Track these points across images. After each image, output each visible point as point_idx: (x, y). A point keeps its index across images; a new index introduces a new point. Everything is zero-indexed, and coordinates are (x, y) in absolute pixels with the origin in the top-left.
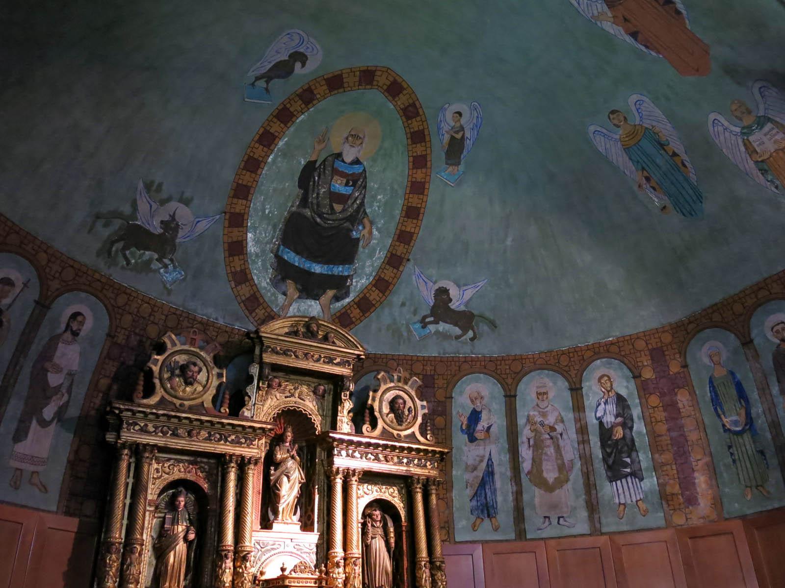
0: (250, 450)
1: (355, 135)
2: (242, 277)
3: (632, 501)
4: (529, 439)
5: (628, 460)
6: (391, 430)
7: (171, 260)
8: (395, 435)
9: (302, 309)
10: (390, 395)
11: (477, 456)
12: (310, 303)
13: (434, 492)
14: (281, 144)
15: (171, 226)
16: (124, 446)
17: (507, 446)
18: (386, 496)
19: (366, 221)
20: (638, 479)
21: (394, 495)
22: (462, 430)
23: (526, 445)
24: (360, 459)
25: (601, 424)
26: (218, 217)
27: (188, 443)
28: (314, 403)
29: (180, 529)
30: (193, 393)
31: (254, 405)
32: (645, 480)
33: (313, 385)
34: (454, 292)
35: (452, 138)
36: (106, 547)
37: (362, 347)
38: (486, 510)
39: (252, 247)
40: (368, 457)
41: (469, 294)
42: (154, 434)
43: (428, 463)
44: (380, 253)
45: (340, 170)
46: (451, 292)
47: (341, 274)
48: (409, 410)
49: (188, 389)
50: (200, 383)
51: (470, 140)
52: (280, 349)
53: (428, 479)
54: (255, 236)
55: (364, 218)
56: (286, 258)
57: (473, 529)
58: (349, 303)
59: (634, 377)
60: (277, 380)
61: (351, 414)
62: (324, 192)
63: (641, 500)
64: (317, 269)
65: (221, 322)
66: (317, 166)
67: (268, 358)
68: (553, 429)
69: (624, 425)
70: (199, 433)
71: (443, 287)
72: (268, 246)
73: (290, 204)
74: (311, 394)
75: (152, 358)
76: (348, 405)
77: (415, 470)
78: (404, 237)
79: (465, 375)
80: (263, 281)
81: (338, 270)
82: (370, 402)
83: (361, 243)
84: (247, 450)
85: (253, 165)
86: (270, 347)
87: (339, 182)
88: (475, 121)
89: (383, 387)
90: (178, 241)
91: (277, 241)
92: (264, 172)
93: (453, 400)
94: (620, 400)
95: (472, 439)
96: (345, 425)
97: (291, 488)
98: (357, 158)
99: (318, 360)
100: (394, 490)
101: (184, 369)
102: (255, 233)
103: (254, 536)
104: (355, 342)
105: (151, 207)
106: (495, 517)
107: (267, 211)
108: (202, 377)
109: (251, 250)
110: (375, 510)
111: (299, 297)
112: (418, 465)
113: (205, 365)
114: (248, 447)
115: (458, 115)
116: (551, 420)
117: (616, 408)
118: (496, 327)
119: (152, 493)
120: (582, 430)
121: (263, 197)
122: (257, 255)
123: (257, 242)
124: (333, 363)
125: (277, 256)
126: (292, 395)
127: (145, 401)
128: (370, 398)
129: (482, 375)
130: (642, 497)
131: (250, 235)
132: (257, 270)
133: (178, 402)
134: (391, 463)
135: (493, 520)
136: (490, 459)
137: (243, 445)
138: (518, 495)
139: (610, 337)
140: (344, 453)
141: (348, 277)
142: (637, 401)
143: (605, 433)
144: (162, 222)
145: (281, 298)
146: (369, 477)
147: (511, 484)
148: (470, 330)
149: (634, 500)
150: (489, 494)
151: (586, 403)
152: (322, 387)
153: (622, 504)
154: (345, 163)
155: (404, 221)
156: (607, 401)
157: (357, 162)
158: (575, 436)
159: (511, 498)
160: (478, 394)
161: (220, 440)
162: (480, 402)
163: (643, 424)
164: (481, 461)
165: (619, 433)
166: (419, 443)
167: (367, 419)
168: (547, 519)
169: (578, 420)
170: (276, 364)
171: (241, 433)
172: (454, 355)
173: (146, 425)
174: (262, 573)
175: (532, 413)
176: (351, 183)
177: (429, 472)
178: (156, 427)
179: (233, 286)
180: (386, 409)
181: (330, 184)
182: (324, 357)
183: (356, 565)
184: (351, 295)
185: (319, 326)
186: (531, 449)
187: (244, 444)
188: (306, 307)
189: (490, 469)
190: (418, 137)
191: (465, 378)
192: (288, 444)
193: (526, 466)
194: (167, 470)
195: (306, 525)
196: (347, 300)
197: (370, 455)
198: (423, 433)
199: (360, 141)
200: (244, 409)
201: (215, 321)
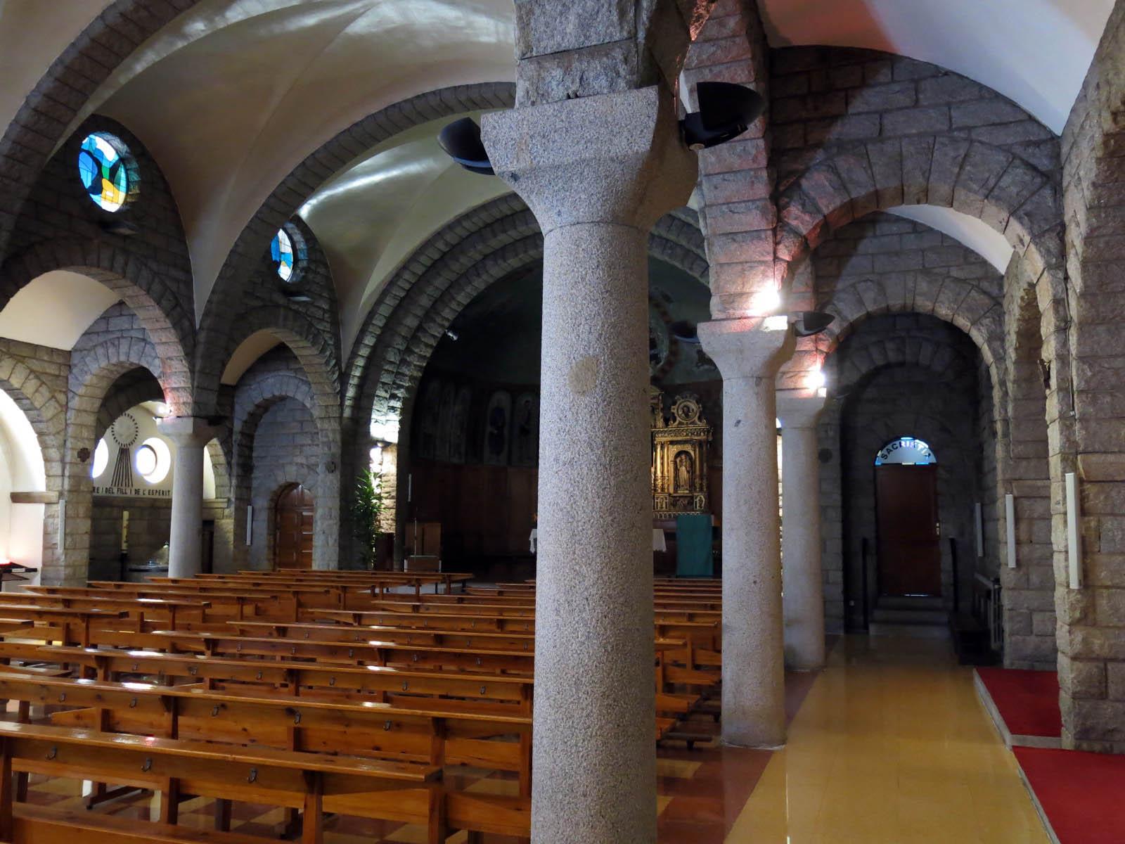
10: (682, 405)
18: (686, 449)
76: (661, 414)
89: (678, 403)
96: (660, 423)
112: (697, 435)
141: (657, 355)
180: (680, 413)
196: (661, 364)
198: (700, 418)
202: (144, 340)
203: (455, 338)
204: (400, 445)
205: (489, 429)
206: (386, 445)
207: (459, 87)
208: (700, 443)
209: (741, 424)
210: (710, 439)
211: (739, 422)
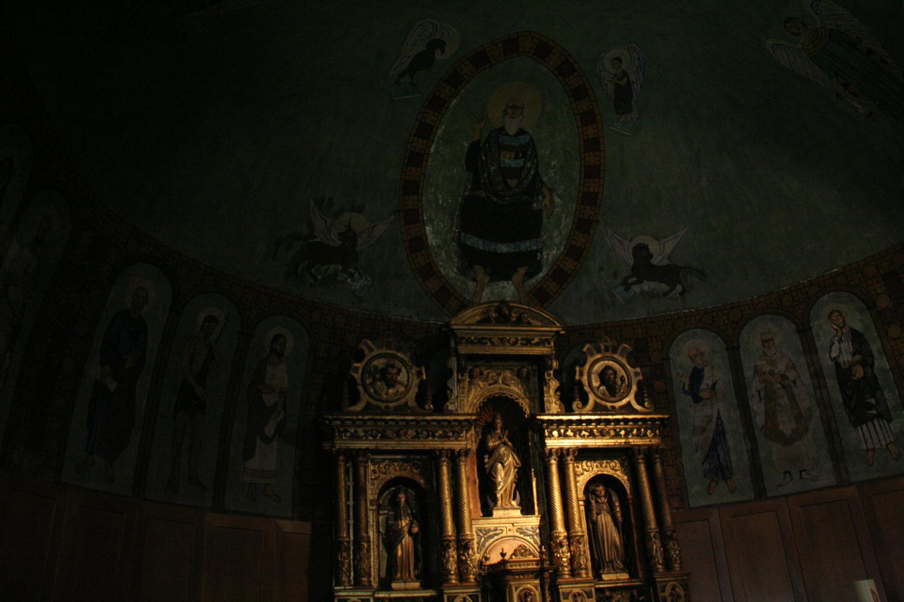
0: (458, 443)
1: (513, 106)
2: (429, 271)
3: (881, 445)
4: (759, 392)
5: (873, 401)
6: (603, 403)
7: (356, 269)
8: (609, 408)
9: (495, 292)
10: (598, 367)
11: (705, 416)
12: (502, 285)
13: (658, 460)
14: (439, 132)
15: (349, 236)
16: (340, 452)
17: (736, 402)
18: (608, 471)
19: (544, 190)
20: (886, 420)
21: (617, 468)
22: (685, 392)
23: (757, 399)
24: (573, 437)
25: (837, 365)
26: (392, 217)
27: (398, 443)
28: (520, 386)
29: (404, 523)
30: (396, 395)
31: (457, 397)
32: (894, 421)
33: (516, 369)
34: (653, 247)
35: (616, 85)
36: (337, 546)
37: (558, 322)
39: (432, 240)
40: (582, 434)
41: (670, 245)
42: (364, 438)
43: (649, 432)
44: (566, 220)
45: (506, 144)
46: (650, 247)
47: (529, 249)
48: (622, 379)
49: (391, 391)
50: (401, 384)
51: (637, 84)
52: (475, 338)
53: (650, 447)
54: (433, 228)
55: (541, 188)
56: (469, 243)
57: (709, 494)
58: (543, 278)
59: (869, 308)
60: (478, 370)
61: (558, 393)
62: (494, 170)
63: (891, 442)
64: (504, 248)
65: (416, 319)
66: (481, 146)
67: (464, 350)
68: (784, 377)
69: (863, 363)
70: (406, 433)
71: (640, 244)
72: (449, 235)
73: (462, 190)
74: (515, 377)
75: (353, 367)
76: (554, 384)
78: (589, 199)
79: (681, 333)
80: (450, 271)
81: (525, 246)
82: (577, 377)
83: (544, 214)
84: (455, 443)
85: (416, 159)
86: (464, 338)
87: (508, 156)
88: (637, 63)
89: (590, 360)
90: (358, 249)
91: (457, 229)
92: (429, 164)
93: (671, 361)
94: (857, 337)
95: (697, 399)
96: (554, 405)
97: (507, 474)
98: (520, 128)
99: (515, 343)
100: (615, 464)
101: (384, 371)
102: (433, 225)
103: (475, 526)
104: (551, 319)
105: (326, 222)
106: (731, 478)
107: (440, 202)
108: (403, 377)
109: (432, 244)
110: (598, 486)
111: (491, 281)
112: (638, 435)
113: (403, 365)
114: (457, 439)
115: (617, 61)
116: (781, 367)
117: (852, 345)
118: (706, 277)
119: (371, 493)
120: (817, 375)
121: (433, 189)
122: (439, 246)
123: (436, 233)
124: (531, 344)
125: (460, 244)
126: (496, 382)
127: (352, 408)
128: (578, 373)
129: (699, 331)
130: (892, 440)
131: (428, 229)
132: (442, 262)
133: (383, 405)
134: (608, 437)
135: (728, 481)
136: (719, 418)
137: (451, 439)
138: (754, 452)
139: (834, 268)
140: (555, 433)
141: (536, 251)
142: (875, 334)
143: (843, 373)
144: (339, 234)
145: (471, 285)
146: (584, 454)
147: (745, 442)
148: (678, 284)
149: (884, 444)
150: (721, 454)
151: (819, 344)
152: (525, 370)
153: (870, 450)
154: (508, 135)
155: (585, 182)
156: (841, 338)
157: (521, 132)
158: (810, 381)
159: (746, 456)
160: (698, 350)
161: (428, 436)
162: (701, 359)
163: (885, 359)
164: (710, 421)
165: (859, 372)
166: (636, 412)
167: (577, 395)
168: (788, 475)
170: (472, 354)
171: (447, 427)
172: (665, 314)
173: (356, 431)
174: (487, 559)
175: (758, 363)
176: (520, 155)
177: (650, 441)
178: (364, 431)
179: (421, 282)
180: (595, 384)
181: (499, 161)
182: (522, 339)
183: (580, 543)
184: (544, 269)
185: (510, 309)
186: (763, 402)
187: (452, 437)
188: (500, 290)
189: (720, 429)
190: (579, 93)
191: (680, 336)
192: (499, 431)
193: (760, 420)
194: (383, 470)
195: (527, 510)
196: (541, 275)
197: (584, 433)
198: (640, 401)
199: (520, 110)
200: (448, 404)
201: (409, 320)
208: (649, 453)
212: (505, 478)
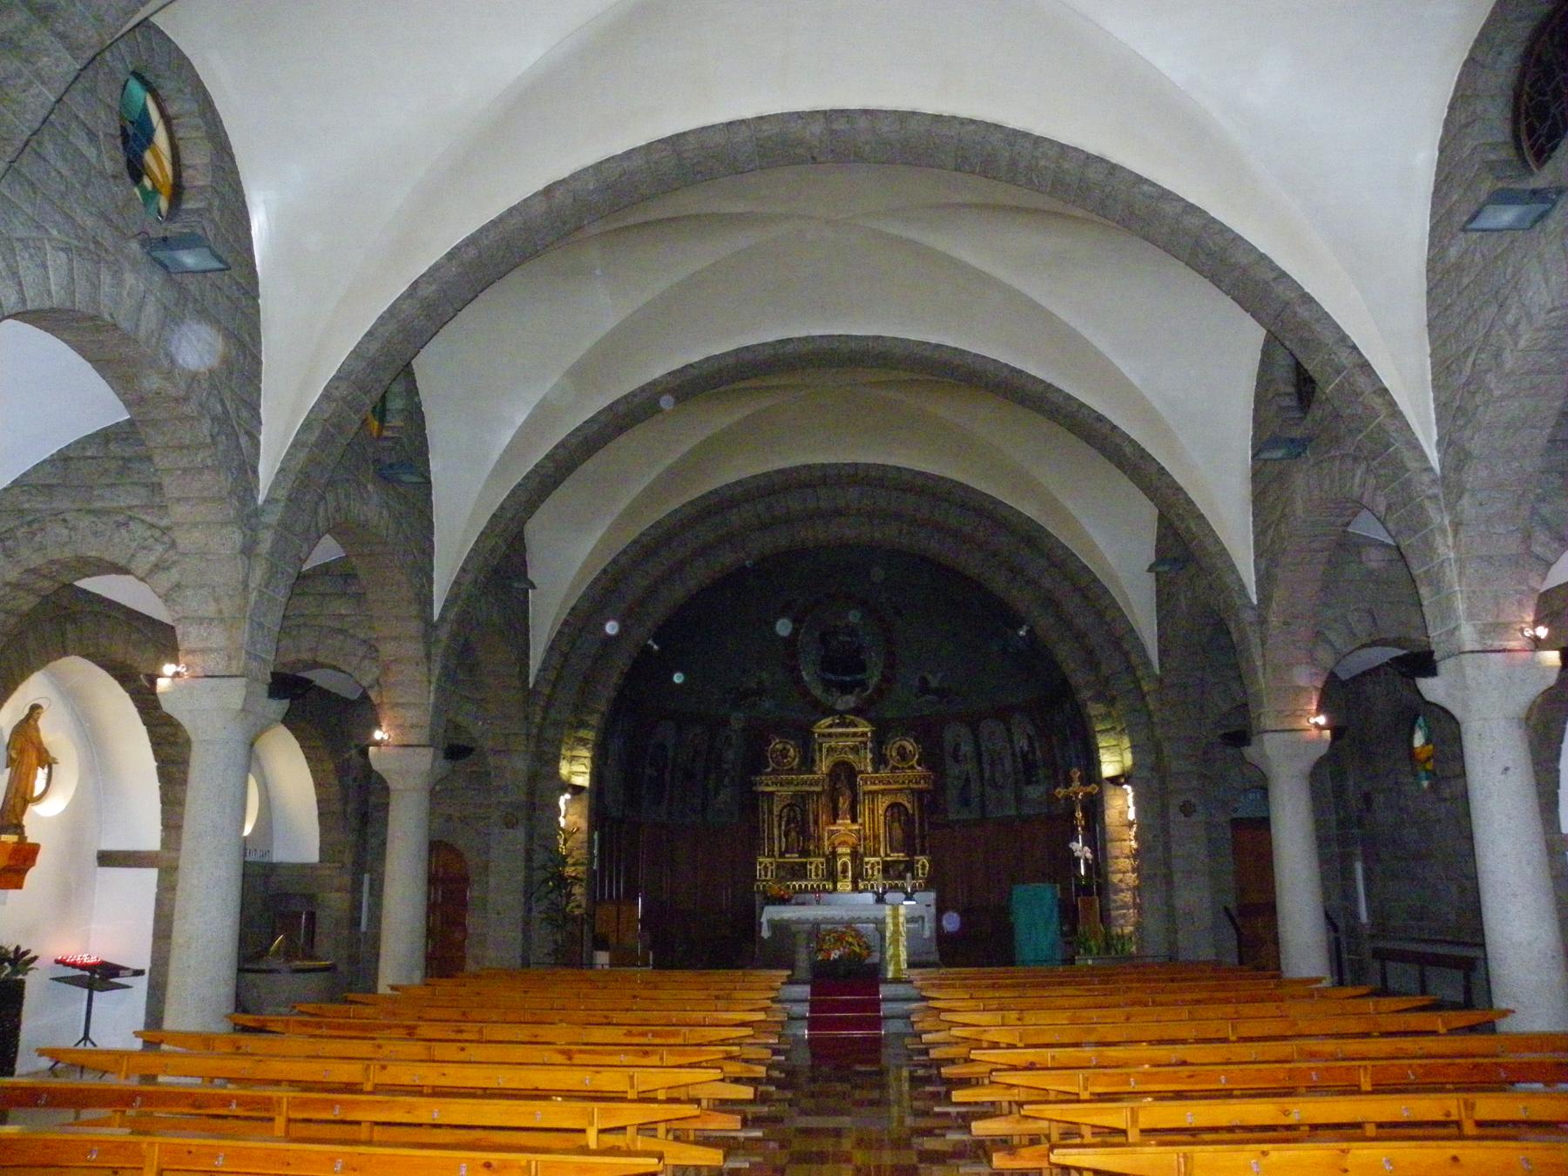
2: (806, 693)
10: (897, 745)
15: (760, 683)
34: (930, 677)
38: (966, 802)
39: (806, 678)
77: (911, 786)
94: (1029, 738)
95: (957, 761)
97: (844, 803)
119: (776, 812)
120: (1013, 754)
131: (803, 673)
143: (1024, 756)
146: (884, 792)
169: (1012, 747)
193: (987, 775)
195: (854, 820)
202: (342, 631)
203: (656, 647)
204: (591, 790)
205: (649, 771)
206: (577, 790)
207: (840, 336)
209: (1510, 772)
210: (931, 787)
211: (1507, 769)
212: (844, 804)
